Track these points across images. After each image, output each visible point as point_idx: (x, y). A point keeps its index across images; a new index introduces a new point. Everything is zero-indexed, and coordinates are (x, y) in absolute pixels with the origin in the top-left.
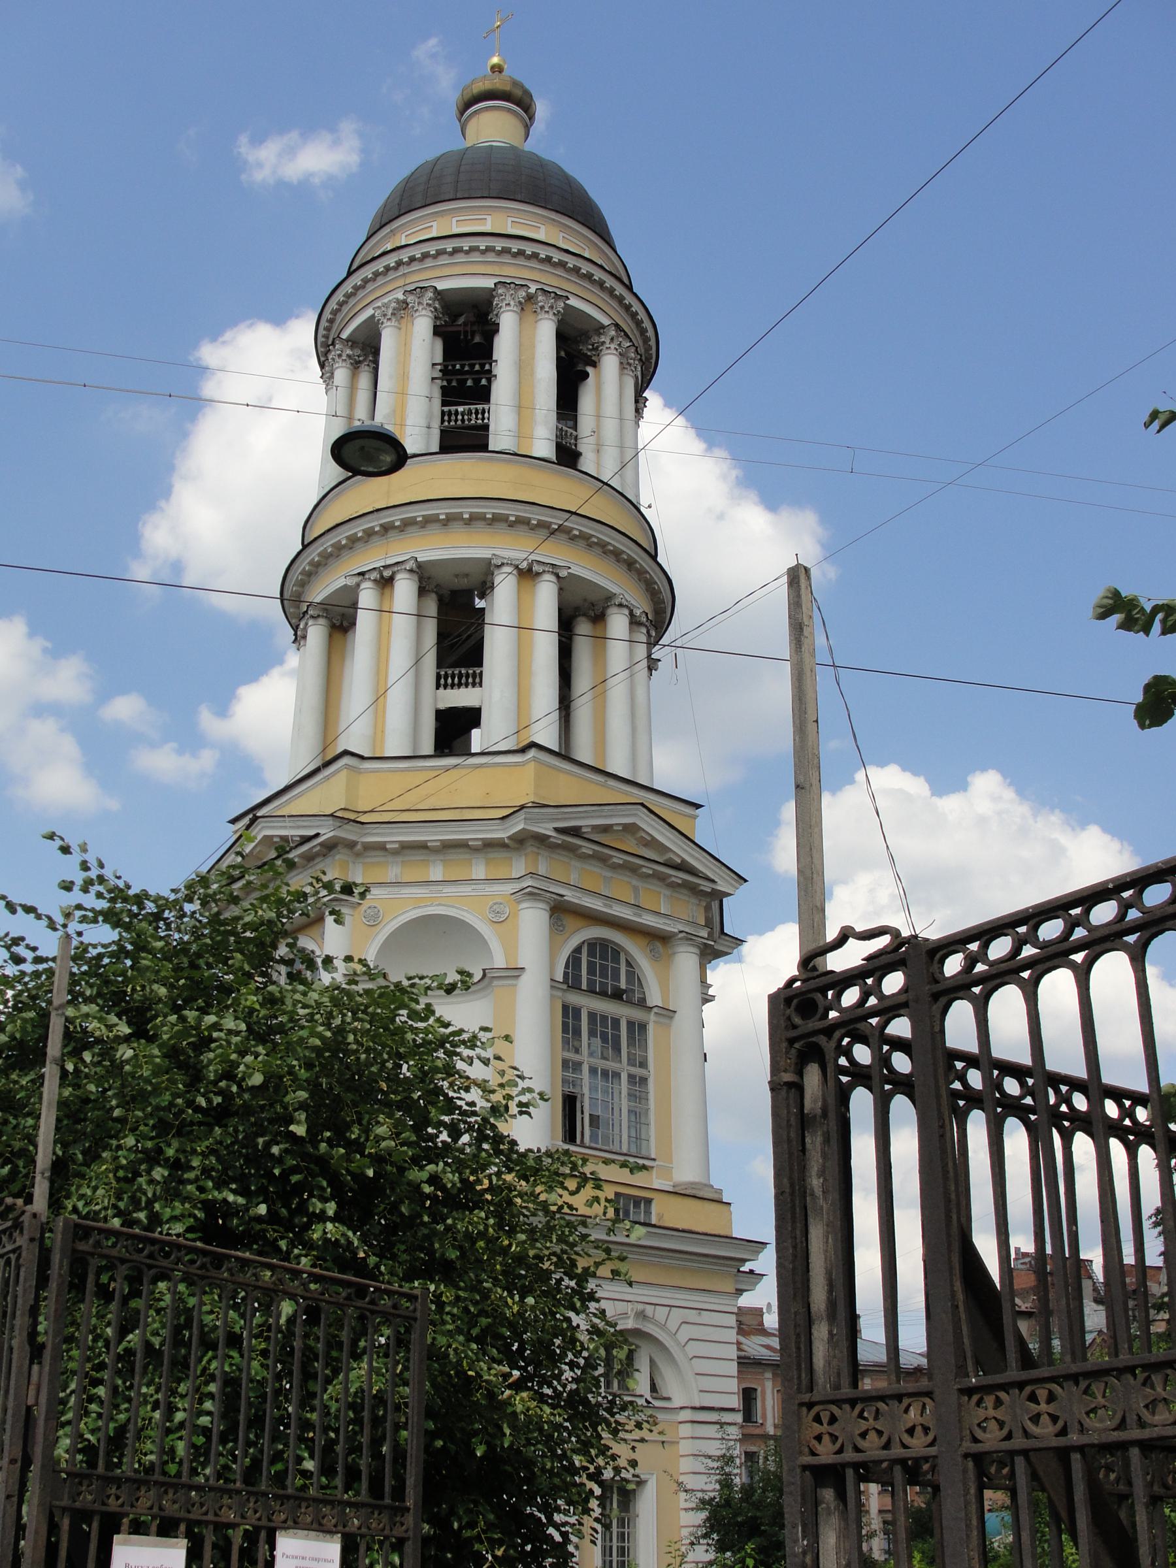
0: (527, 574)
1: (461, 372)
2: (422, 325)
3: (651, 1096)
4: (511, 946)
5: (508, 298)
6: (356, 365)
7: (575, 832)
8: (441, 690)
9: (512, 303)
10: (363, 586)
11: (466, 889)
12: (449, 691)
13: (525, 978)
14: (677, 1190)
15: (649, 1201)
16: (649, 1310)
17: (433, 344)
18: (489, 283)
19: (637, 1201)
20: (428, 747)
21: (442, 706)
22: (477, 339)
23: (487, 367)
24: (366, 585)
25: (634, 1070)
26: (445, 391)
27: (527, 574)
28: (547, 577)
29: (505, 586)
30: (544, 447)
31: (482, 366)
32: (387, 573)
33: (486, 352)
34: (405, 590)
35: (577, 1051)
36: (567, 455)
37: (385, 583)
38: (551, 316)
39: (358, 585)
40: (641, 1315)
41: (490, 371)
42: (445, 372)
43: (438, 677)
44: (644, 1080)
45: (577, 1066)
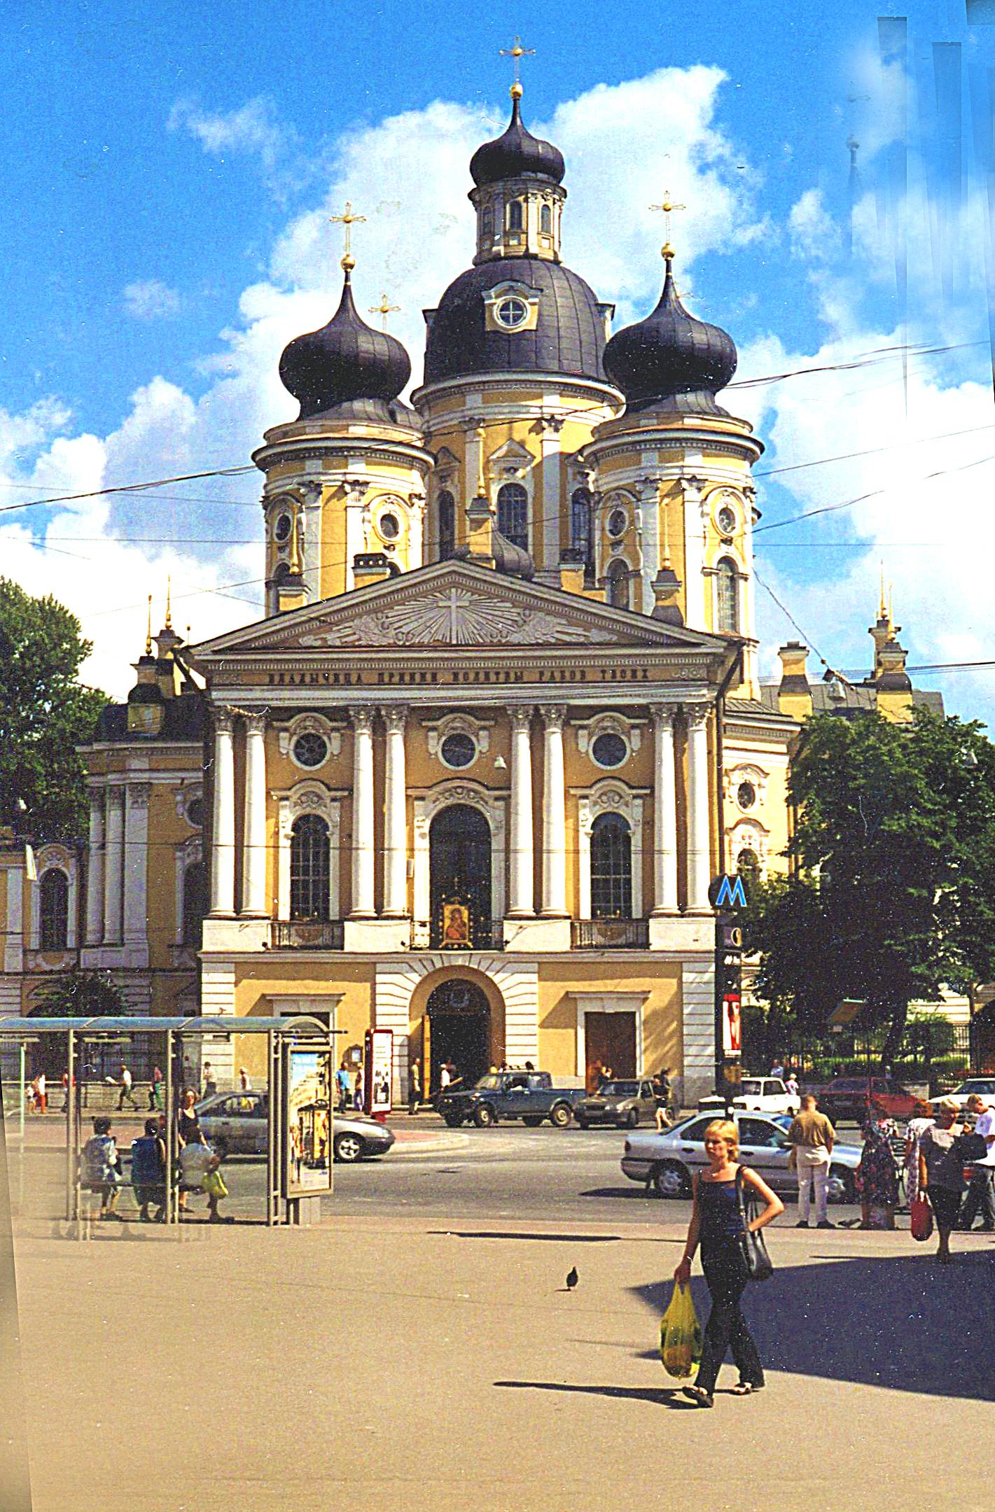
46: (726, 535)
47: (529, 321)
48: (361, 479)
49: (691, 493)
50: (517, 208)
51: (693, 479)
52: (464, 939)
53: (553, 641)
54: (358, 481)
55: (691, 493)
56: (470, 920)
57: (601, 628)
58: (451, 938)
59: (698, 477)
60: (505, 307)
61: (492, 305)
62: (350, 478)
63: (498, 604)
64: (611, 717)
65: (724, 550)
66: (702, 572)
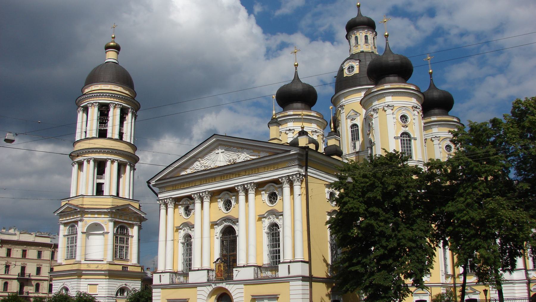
0: (113, 162)
1: (103, 119)
2: (96, 109)
3: (129, 250)
4: (108, 228)
5: (112, 105)
6: (83, 112)
7: (118, 210)
8: (98, 180)
9: (113, 106)
10: (84, 161)
11: (101, 219)
12: (99, 180)
13: (109, 233)
14: (133, 265)
15: (127, 267)
16: (127, 284)
17: (98, 112)
18: (109, 102)
19: (126, 267)
20: (95, 194)
21: (97, 182)
22: (106, 113)
23: (107, 118)
24: (85, 161)
25: (126, 246)
26: (100, 123)
27: (113, 162)
28: (116, 162)
29: (109, 163)
30: (117, 136)
31: (107, 118)
32: (89, 160)
33: (107, 115)
34: (92, 163)
35: (118, 244)
36: (121, 134)
37: (88, 162)
38: (119, 108)
39: (84, 161)
40: (126, 284)
41: (108, 119)
42: (100, 119)
43: (97, 177)
44: (128, 247)
45: (117, 246)
46: (404, 124)
47: (356, 71)
48: (291, 128)
49: (389, 111)
50: (356, 38)
51: (388, 106)
52: (222, 276)
53: (249, 159)
54: (289, 129)
55: (389, 111)
56: (223, 269)
57: (263, 151)
58: (218, 276)
59: (390, 105)
60: (349, 68)
61: (345, 68)
62: (288, 129)
63: (233, 149)
64: (272, 185)
65: (403, 130)
66: (394, 138)
